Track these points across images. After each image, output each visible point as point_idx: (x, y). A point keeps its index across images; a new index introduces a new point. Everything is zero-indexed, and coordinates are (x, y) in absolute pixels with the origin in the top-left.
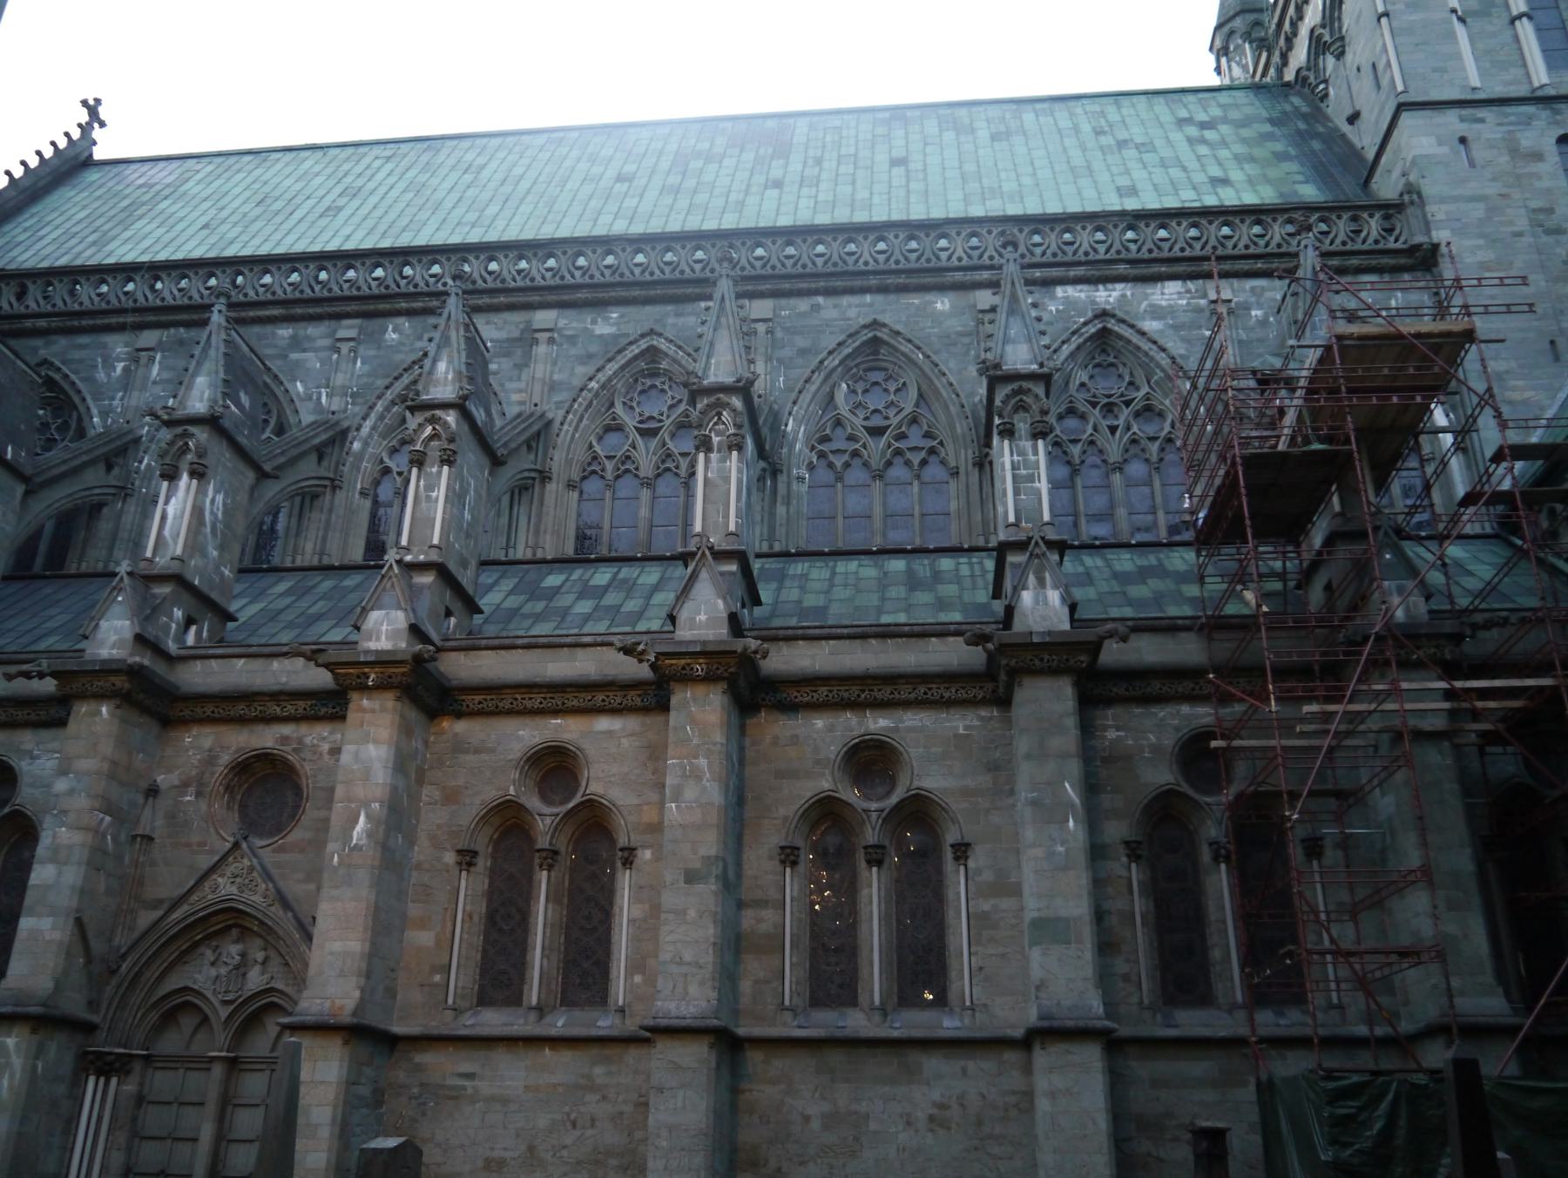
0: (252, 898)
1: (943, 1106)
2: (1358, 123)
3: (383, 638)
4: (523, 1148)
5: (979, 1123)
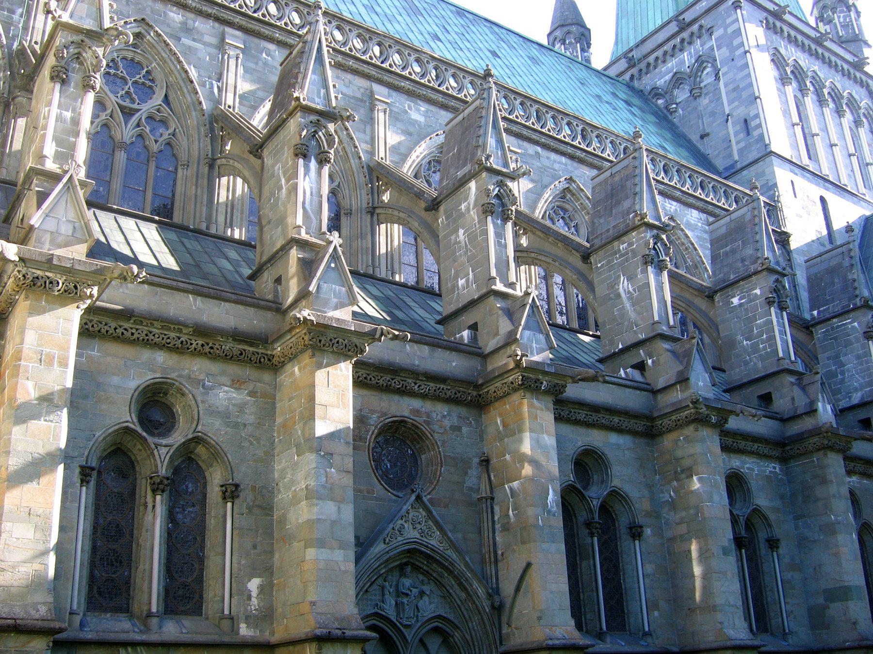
0: (431, 542)
2: (706, 139)
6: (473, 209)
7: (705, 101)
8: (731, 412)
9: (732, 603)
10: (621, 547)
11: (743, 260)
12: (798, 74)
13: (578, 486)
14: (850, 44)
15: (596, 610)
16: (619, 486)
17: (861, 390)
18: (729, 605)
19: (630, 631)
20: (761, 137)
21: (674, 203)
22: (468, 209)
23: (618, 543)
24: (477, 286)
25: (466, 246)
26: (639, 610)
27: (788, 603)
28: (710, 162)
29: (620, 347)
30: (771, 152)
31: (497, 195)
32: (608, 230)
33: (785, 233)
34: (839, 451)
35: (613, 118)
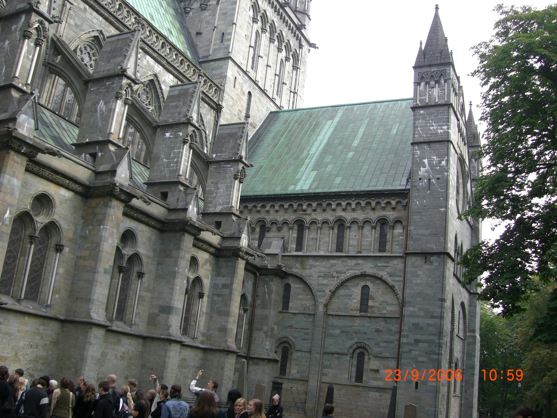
1: (124, 353)
2: (199, 36)
3: (25, 129)
4: (14, 353)
5: (130, 359)
6: (19, 31)
7: (206, 13)
8: (134, 196)
9: (100, 300)
10: (48, 254)
11: (179, 113)
12: (264, 17)
13: (31, 213)
14: (300, 14)
15: (21, 286)
16: (57, 219)
17: (222, 205)
18: (98, 301)
19: (39, 302)
20: (228, 47)
21: (161, 67)
22: (16, 29)
23: (47, 252)
24: (5, 78)
25: (7, 52)
26: (48, 292)
27: (138, 308)
28: (196, 50)
29: (87, 140)
30: (230, 57)
31: (36, 28)
32: (104, 71)
33: (220, 105)
34: (192, 234)
35: (147, 3)
